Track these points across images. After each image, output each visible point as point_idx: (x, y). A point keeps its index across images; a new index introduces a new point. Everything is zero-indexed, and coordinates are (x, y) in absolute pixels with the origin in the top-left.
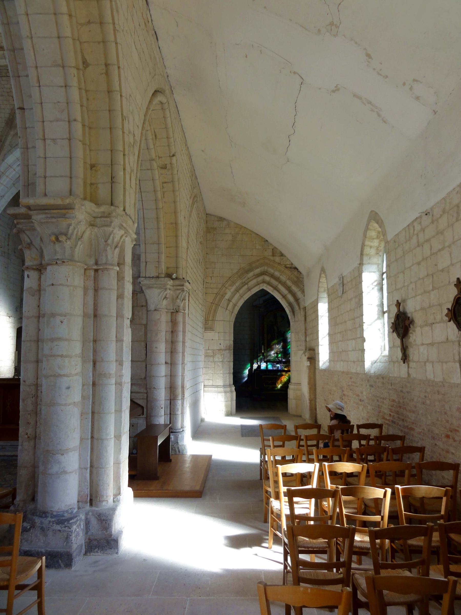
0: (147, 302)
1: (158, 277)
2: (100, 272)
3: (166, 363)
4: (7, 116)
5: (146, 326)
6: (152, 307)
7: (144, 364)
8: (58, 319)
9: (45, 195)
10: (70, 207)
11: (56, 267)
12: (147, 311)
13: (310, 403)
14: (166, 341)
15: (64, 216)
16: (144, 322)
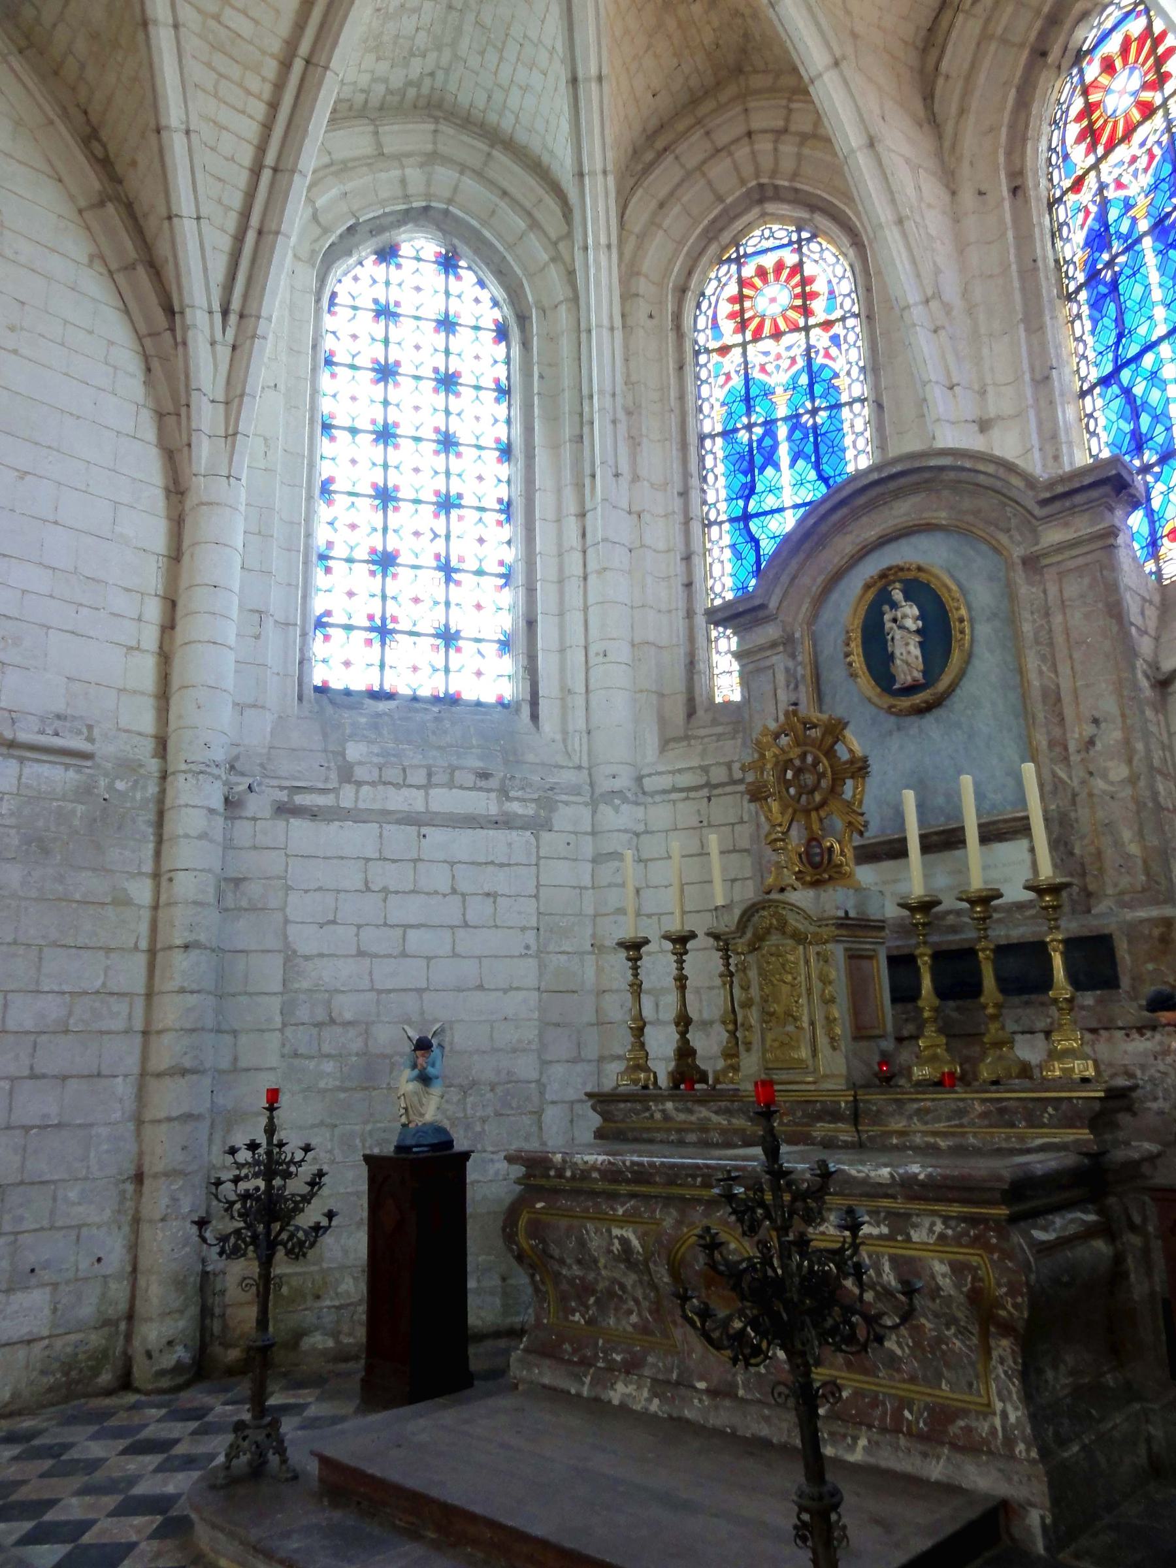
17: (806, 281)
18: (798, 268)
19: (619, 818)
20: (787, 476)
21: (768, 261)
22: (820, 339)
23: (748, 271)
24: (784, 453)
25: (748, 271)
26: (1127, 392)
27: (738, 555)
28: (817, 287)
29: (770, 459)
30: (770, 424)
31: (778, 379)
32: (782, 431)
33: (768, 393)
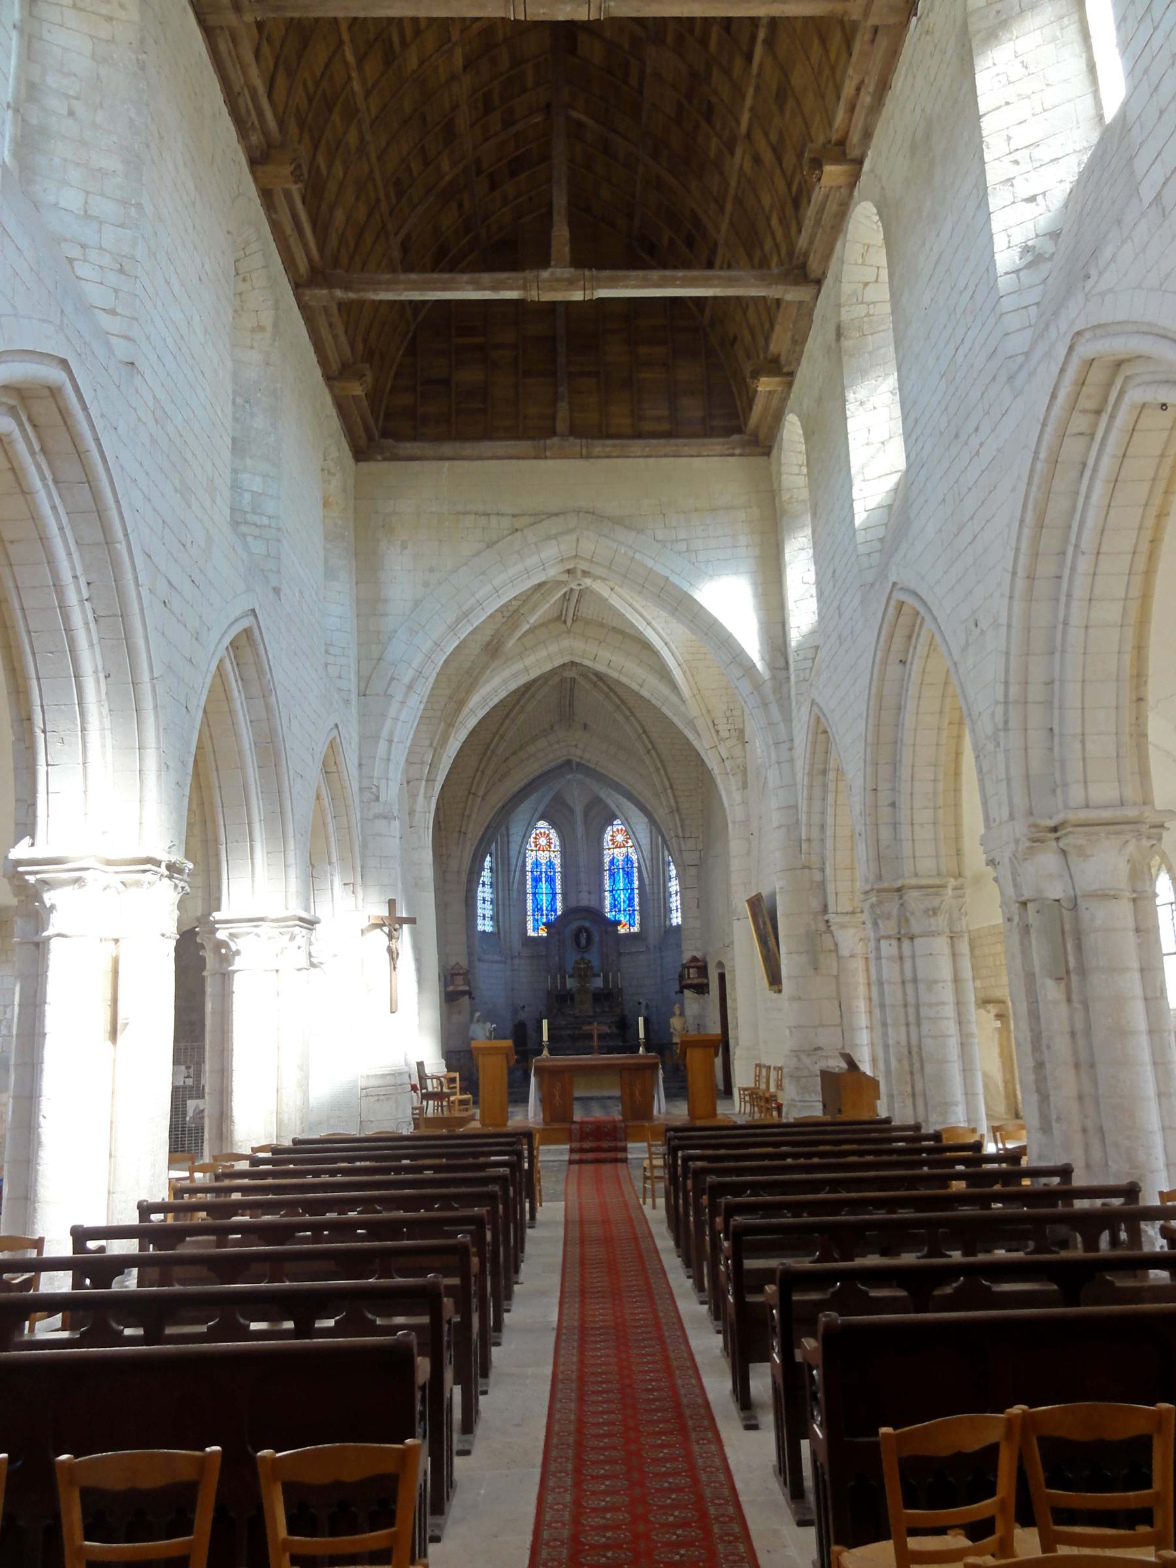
0: (836, 945)
1: (853, 913)
2: (954, 939)
3: (867, 1027)
4: (488, 639)
5: (837, 977)
6: (845, 952)
7: (839, 1030)
8: (940, 985)
9: (916, 875)
10: (944, 886)
11: (932, 938)
12: (839, 958)
13: (1006, 1087)
14: (864, 998)
15: (937, 894)
16: (835, 972)
17: (550, 839)
18: (548, 835)
19: (516, 961)
20: (544, 886)
21: (542, 830)
22: (553, 855)
23: (538, 832)
24: (544, 879)
25: (538, 832)
26: (614, 896)
27: (533, 902)
28: (552, 841)
29: (541, 880)
30: (541, 872)
31: (543, 862)
32: (544, 875)
33: (541, 864)
